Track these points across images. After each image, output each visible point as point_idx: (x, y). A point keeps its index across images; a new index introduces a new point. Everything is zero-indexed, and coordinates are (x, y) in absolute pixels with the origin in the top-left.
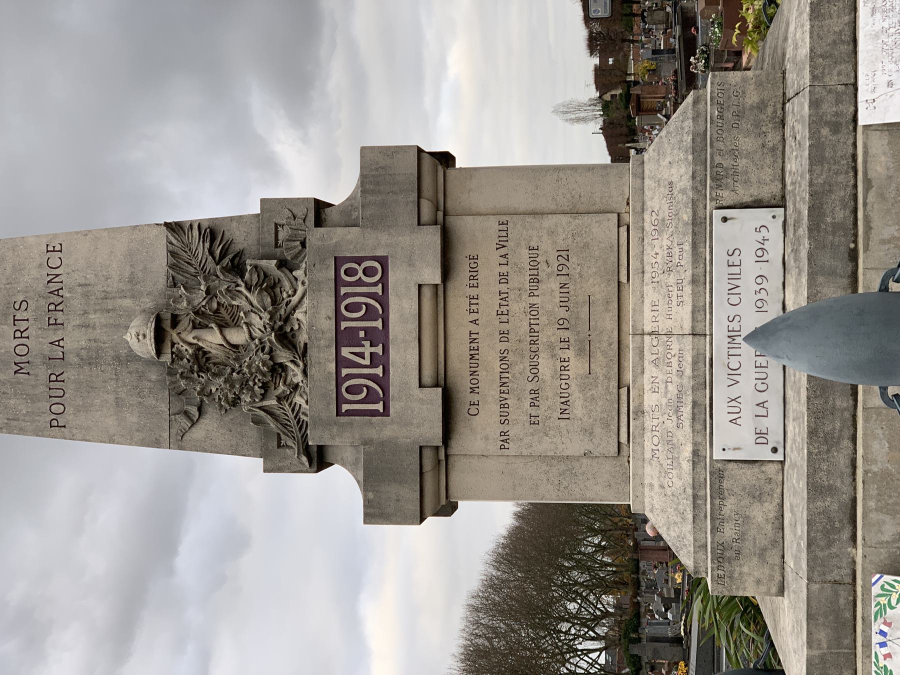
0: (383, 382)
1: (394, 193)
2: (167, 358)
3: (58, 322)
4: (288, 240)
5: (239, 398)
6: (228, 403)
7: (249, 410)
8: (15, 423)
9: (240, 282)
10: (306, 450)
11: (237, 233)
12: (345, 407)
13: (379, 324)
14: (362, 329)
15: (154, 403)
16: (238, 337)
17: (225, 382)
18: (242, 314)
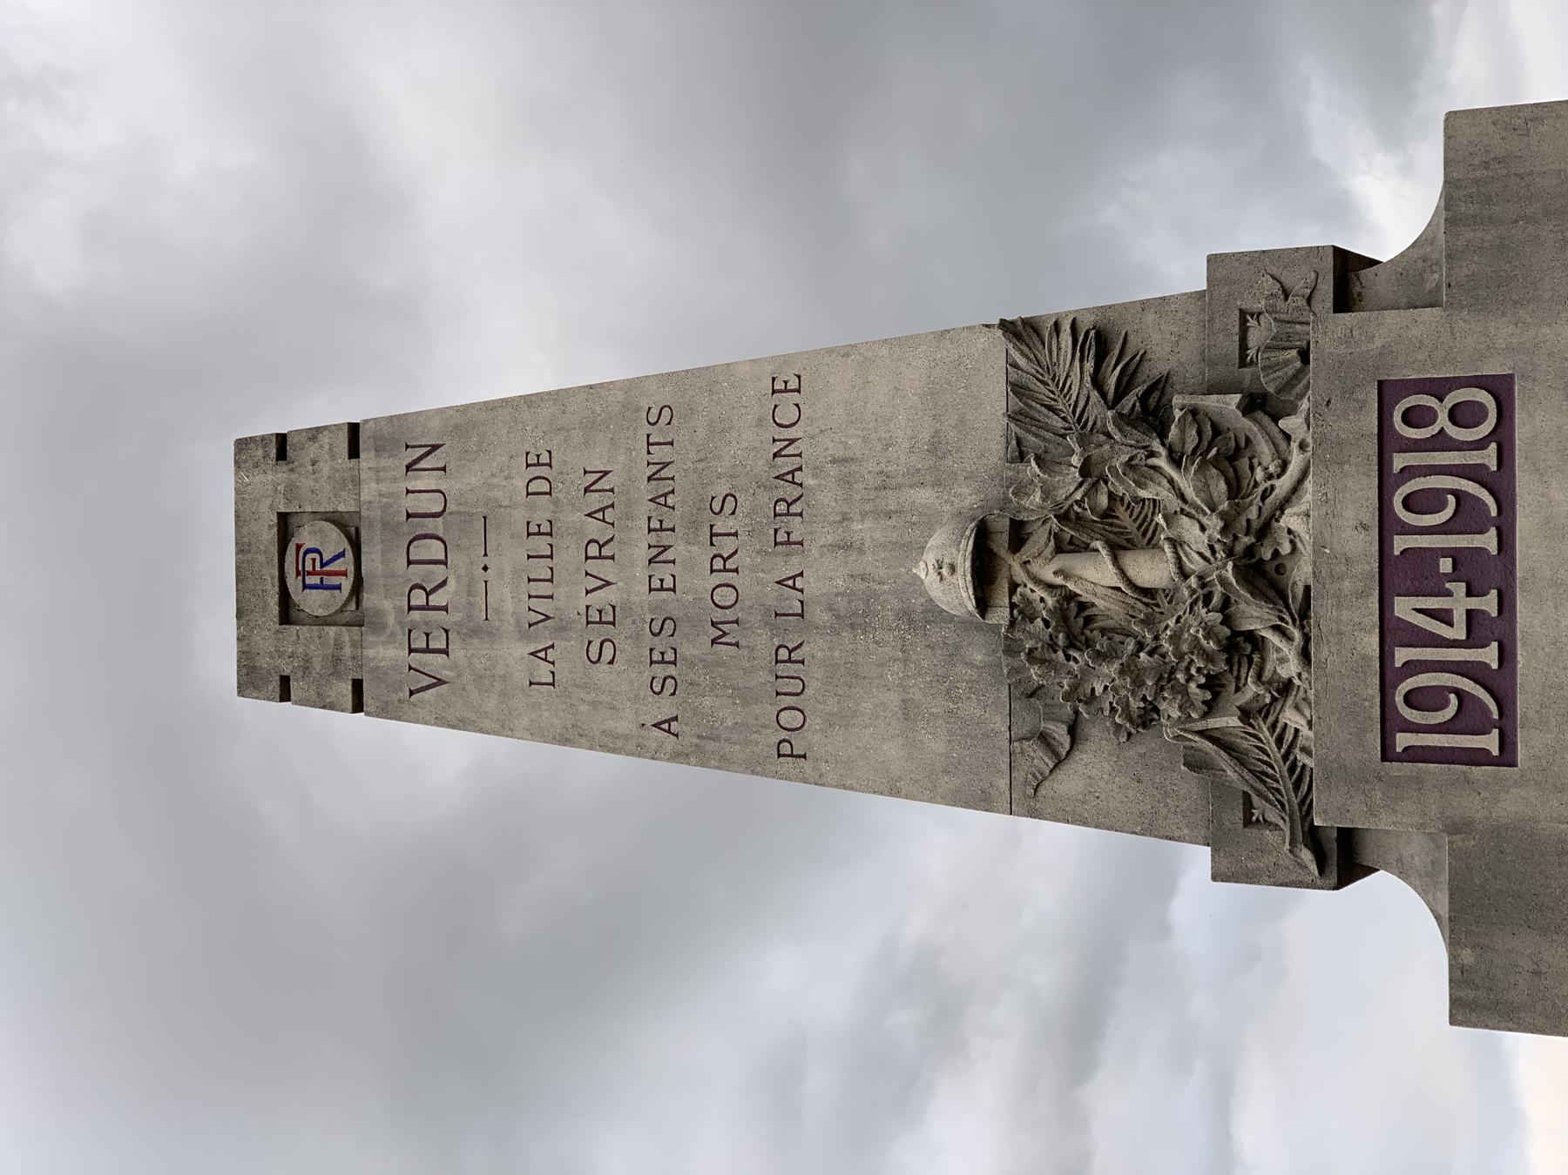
0: (1500, 683)
1: (1529, 219)
2: (1000, 615)
3: (793, 538)
4: (1269, 348)
5: (1157, 710)
6: (1131, 720)
7: (1178, 737)
8: (711, 745)
9: (1156, 445)
10: (1313, 837)
11: (1156, 337)
12: (1403, 740)
13: (1488, 541)
14: (1445, 552)
15: (979, 712)
16: (1152, 570)
17: (1122, 672)
18: (1159, 519)
